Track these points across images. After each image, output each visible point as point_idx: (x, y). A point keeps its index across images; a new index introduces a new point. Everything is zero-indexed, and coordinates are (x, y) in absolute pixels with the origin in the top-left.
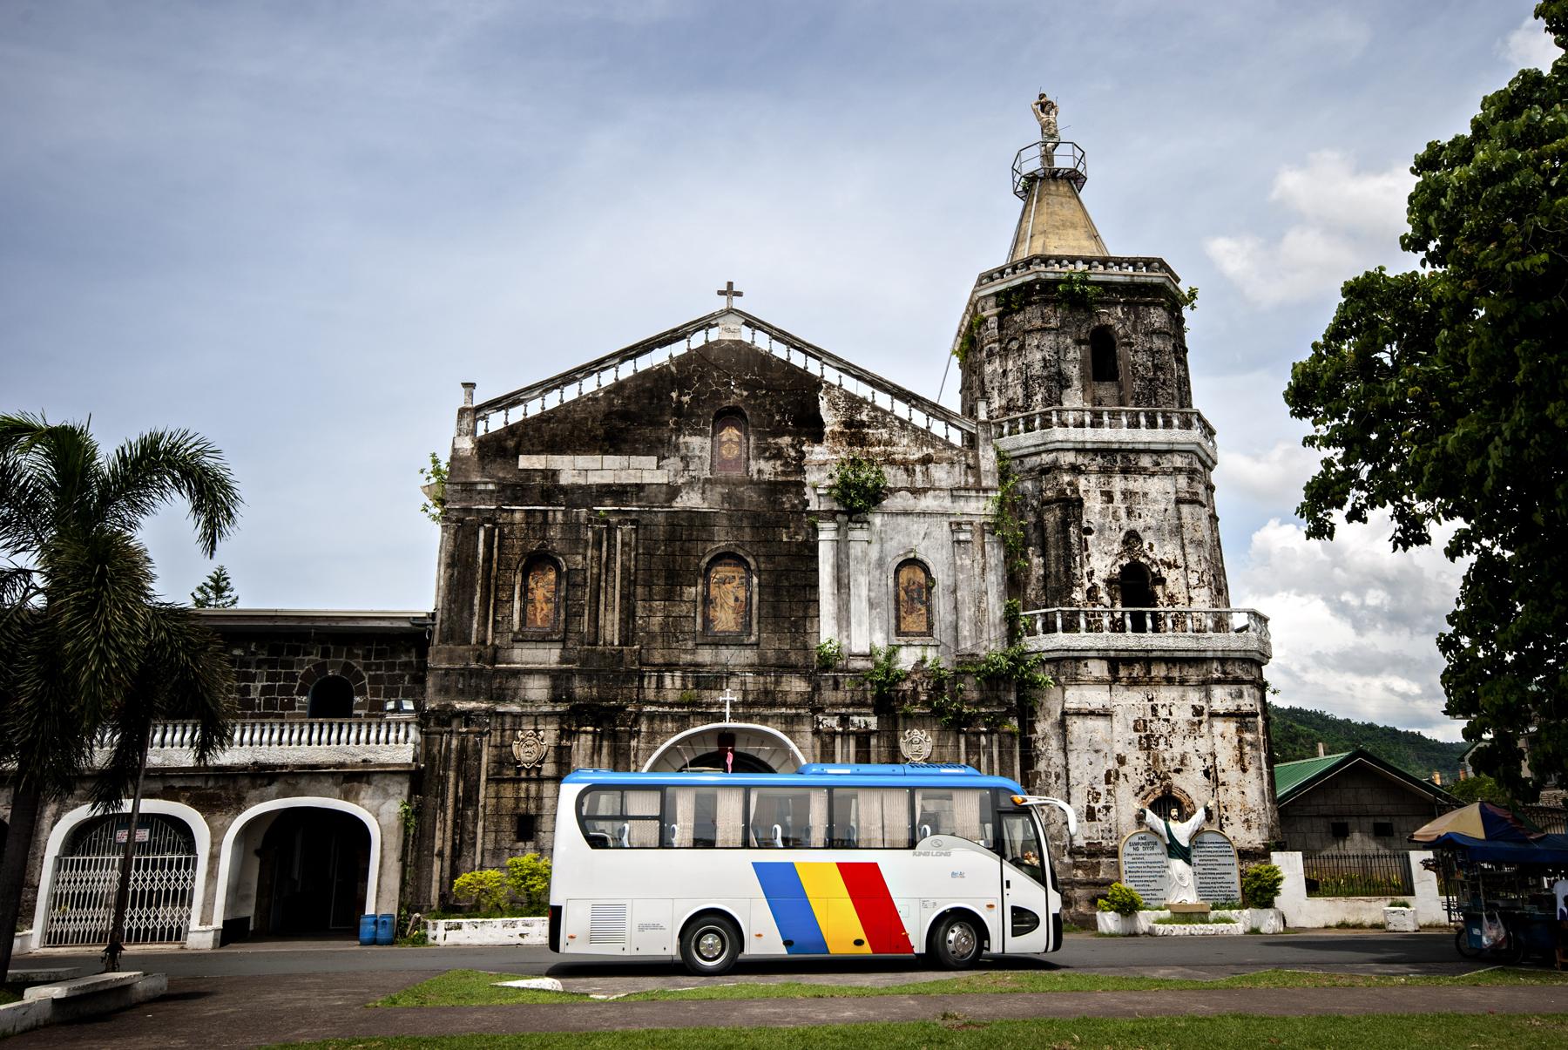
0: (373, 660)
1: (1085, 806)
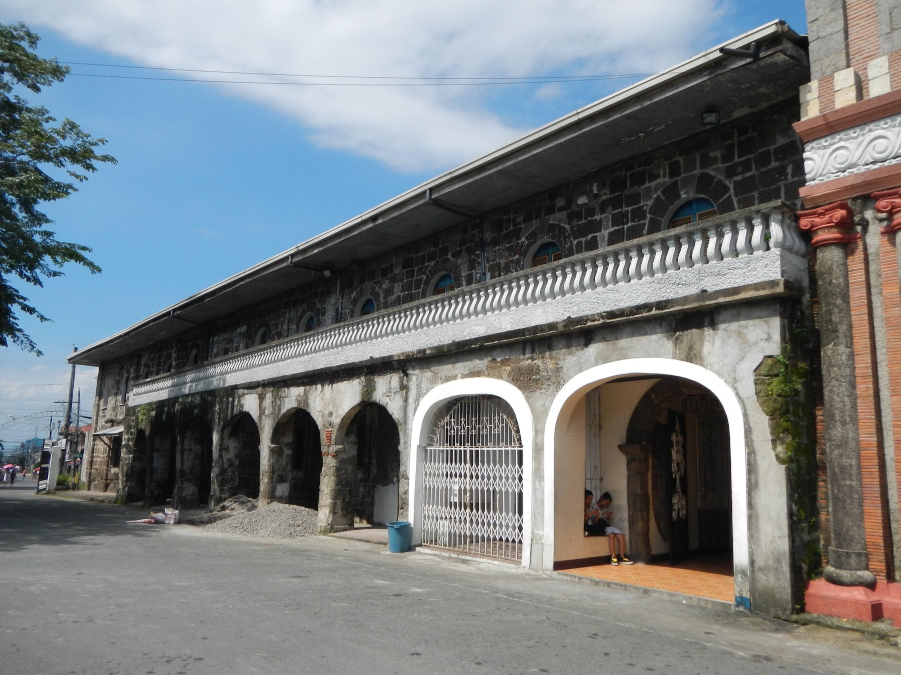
0: (737, 160)
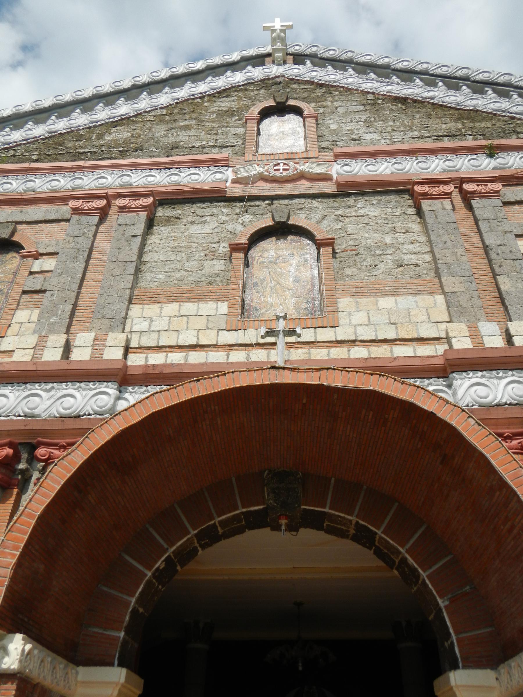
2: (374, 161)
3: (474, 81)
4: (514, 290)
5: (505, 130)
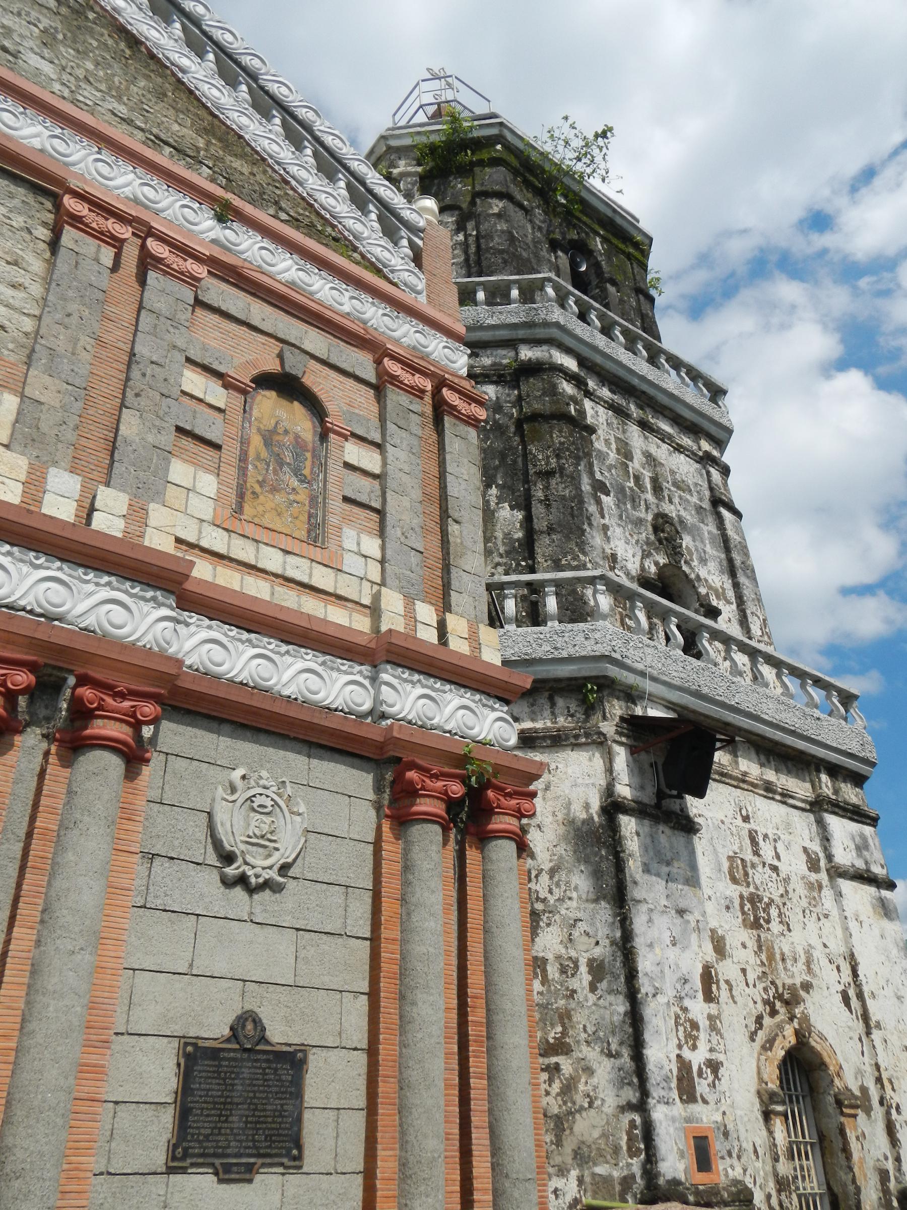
1: (673, 1057)
2: (22, 110)
3: (262, 88)
4: (137, 441)
5: (264, 193)
